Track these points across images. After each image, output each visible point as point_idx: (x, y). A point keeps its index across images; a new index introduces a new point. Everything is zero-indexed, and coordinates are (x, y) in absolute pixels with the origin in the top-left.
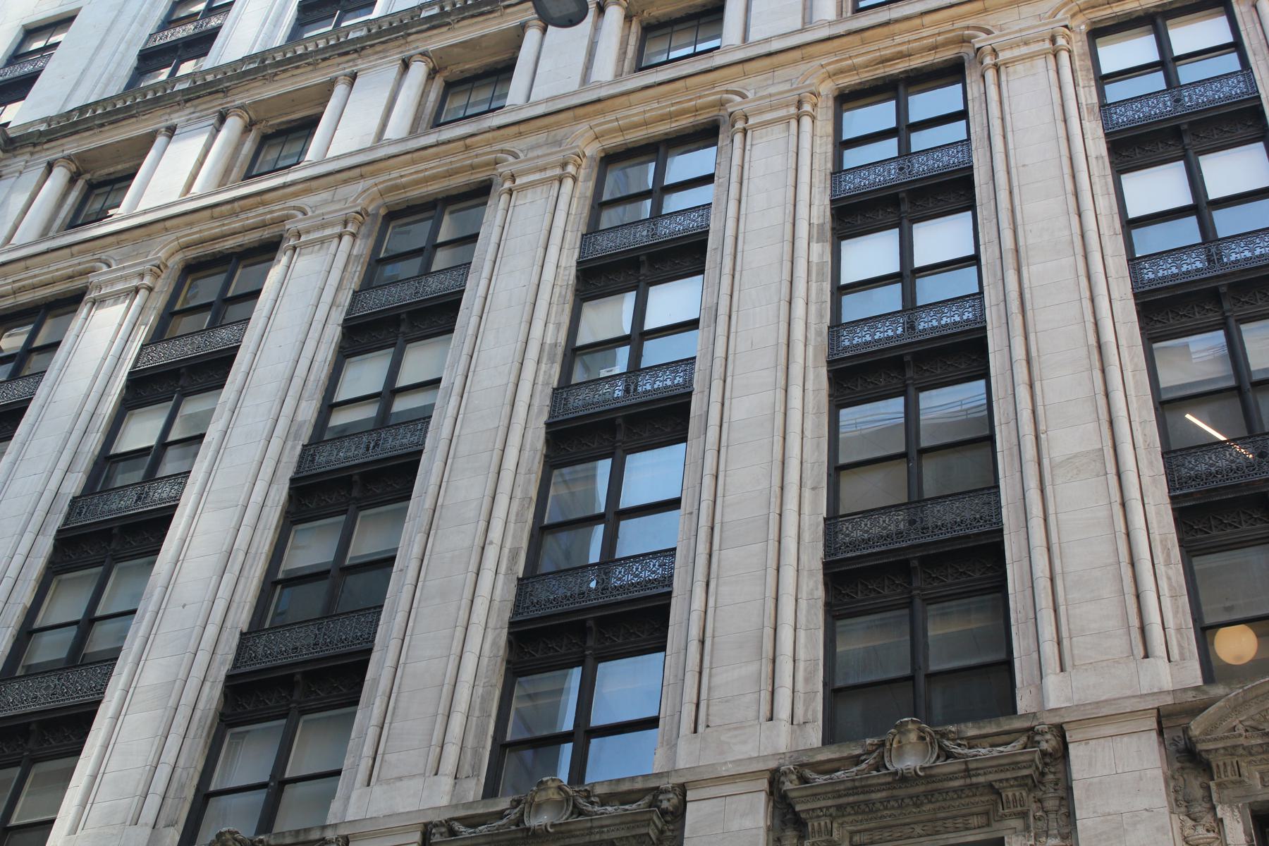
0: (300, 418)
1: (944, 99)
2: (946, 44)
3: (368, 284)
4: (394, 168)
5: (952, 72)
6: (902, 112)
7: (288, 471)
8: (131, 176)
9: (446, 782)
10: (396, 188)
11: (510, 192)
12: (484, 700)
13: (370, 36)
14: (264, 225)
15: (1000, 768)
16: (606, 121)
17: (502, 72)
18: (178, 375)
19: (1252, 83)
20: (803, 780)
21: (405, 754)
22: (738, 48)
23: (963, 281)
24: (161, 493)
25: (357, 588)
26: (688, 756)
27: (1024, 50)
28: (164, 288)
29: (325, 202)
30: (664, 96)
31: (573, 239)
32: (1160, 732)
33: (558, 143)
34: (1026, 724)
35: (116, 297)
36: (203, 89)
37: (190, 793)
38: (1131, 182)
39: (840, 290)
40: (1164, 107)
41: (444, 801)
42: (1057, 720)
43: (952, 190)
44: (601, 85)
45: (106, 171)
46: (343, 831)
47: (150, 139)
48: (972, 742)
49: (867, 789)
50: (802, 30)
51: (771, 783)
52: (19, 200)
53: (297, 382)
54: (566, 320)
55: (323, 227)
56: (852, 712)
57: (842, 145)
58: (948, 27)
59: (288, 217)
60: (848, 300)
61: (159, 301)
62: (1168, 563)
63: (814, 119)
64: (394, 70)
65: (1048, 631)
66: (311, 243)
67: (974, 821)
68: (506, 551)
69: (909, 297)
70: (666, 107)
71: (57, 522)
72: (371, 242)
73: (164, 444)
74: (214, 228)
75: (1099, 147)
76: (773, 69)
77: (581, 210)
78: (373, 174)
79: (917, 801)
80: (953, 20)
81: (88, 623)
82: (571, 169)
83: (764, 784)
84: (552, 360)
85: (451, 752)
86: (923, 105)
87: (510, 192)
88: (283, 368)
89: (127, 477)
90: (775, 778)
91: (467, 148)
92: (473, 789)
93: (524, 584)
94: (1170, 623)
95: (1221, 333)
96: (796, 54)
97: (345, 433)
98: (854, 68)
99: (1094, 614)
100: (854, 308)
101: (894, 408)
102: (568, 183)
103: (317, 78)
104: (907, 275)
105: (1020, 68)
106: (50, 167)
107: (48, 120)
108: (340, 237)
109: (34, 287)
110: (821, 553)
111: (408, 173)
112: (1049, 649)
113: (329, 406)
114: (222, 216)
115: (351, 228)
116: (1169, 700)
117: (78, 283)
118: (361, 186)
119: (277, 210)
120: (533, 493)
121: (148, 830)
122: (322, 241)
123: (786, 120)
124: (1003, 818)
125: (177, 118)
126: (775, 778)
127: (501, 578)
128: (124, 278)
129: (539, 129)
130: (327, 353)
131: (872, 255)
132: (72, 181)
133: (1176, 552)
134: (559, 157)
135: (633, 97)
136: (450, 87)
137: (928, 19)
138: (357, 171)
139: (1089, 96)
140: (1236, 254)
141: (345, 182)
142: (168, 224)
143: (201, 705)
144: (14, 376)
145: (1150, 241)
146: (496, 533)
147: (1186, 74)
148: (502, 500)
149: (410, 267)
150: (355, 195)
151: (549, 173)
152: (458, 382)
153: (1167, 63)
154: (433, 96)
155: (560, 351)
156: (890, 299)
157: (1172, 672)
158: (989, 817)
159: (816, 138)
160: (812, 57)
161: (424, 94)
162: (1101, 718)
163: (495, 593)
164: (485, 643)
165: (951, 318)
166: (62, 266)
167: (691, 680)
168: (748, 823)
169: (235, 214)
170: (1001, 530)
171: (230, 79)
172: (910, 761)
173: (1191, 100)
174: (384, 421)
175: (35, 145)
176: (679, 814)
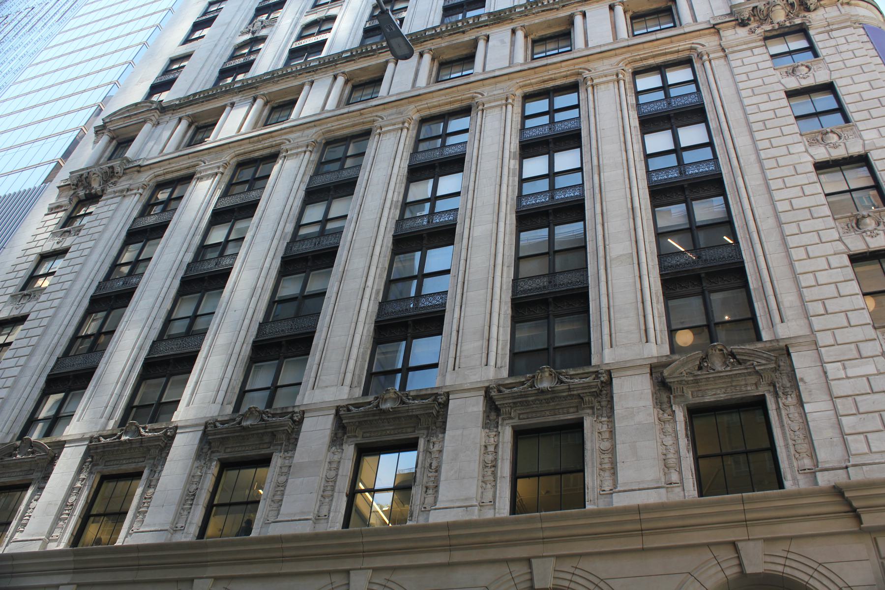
0: (286, 230)
1: (570, 99)
3: (317, 173)
5: (574, 87)
6: (551, 104)
7: (280, 254)
8: (215, 124)
9: (346, 389)
10: (330, 131)
11: (380, 134)
12: (364, 354)
13: (320, 65)
14: (272, 146)
15: (583, 388)
16: (422, 104)
17: (377, 81)
18: (234, 212)
19: (701, 97)
20: (499, 391)
21: (329, 376)
22: (481, 74)
23: (575, 179)
24: (226, 262)
25: (309, 305)
26: (450, 380)
27: (605, 79)
28: (228, 173)
29: (299, 137)
30: (448, 94)
31: (407, 155)
32: (651, 374)
33: (401, 113)
34: (595, 370)
35: (208, 177)
36: (247, 87)
37: (237, 391)
38: (649, 138)
39: (522, 181)
40: (664, 106)
41: (345, 397)
42: (608, 368)
43: (571, 139)
44: (420, 88)
46: (302, 408)
47: (223, 108)
48: (572, 377)
49: (526, 396)
50: (509, 67)
51: (486, 392)
52: (166, 134)
53: (285, 215)
54: (402, 190)
55: (298, 148)
56: (521, 363)
57: (525, 118)
58: (572, 68)
59: (282, 143)
60: (525, 185)
61: (226, 179)
62: (658, 302)
63: (513, 106)
64: (330, 79)
65: (606, 330)
66: (293, 155)
67: (572, 410)
68: (374, 291)
69: (552, 185)
71: (181, 274)
72: (318, 154)
73: (227, 241)
74: (250, 147)
75: (635, 123)
76: (496, 83)
77: (410, 143)
78: (320, 125)
79: (548, 401)
80: (574, 65)
81: (195, 317)
82: (406, 125)
83: (483, 393)
84: (396, 208)
85: (349, 376)
86: (561, 101)
87: (380, 134)
88: (279, 209)
89: (212, 255)
90: (487, 390)
91: (361, 114)
92: (358, 392)
93: (382, 305)
94: (658, 328)
95: (684, 205)
96: (506, 77)
97: (306, 238)
98: (531, 84)
99: (626, 323)
100: (528, 189)
101: (545, 232)
102: (405, 131)
103: (296, 83)
104: (551, 175)
105: (602, 86)
106: (180, 120)
107: (179, 99)
108: (305, 152)
109: (172, 172)
110: (510, 294)
111: (334, 125)
112: (606, 338)
113: (299, 226)
114: (253, 142)
115: (310, 148)
116: (655, 361)
117: (191, 171)
118: (314, 130)
119: (278, 140)
120: (387, 266)
121: (220, 406)
122: (297, 154)
123: (501, 106)
124: (584, 409)
125: (235, 99)
126: (487, 390)
127: (372, 302)
129: (392, 107)
130: (298, 202)
131: (536, 166)
132: (190, 126)
133: (661, 298)
134: (401, 119)
136: (355, 88)
137: (564, 64)
138: (313, 124)
139: (632, 100)
140: (692, 171)
141: (308, 128)
143: (242, 354)
144: (164, 210)
146: (370, 283)
147: (674, 92)
148: (373, 269)
149: (336, 166)
150: (312, 134)
151: (397, 126)
152: (355, 216)
153: (665, 87)
154: (347, 91)
155: (400, 204)
156: (544, 185)
157: (657, 349)
158: (578, 408)
159: (513, 114)
160: (513, 79)
161: (343, 91)
162: (627, 368)
163: (369, 309)
164: (364, 330)
165: (570, 194)
166: (185, 163)
167: (453, 348)
168: (475, 409)
170: (588, 287)
171: (258, 82)
172: (545, 384)
173: (675, 104)
174: (322, 233)
176: (446, 405)
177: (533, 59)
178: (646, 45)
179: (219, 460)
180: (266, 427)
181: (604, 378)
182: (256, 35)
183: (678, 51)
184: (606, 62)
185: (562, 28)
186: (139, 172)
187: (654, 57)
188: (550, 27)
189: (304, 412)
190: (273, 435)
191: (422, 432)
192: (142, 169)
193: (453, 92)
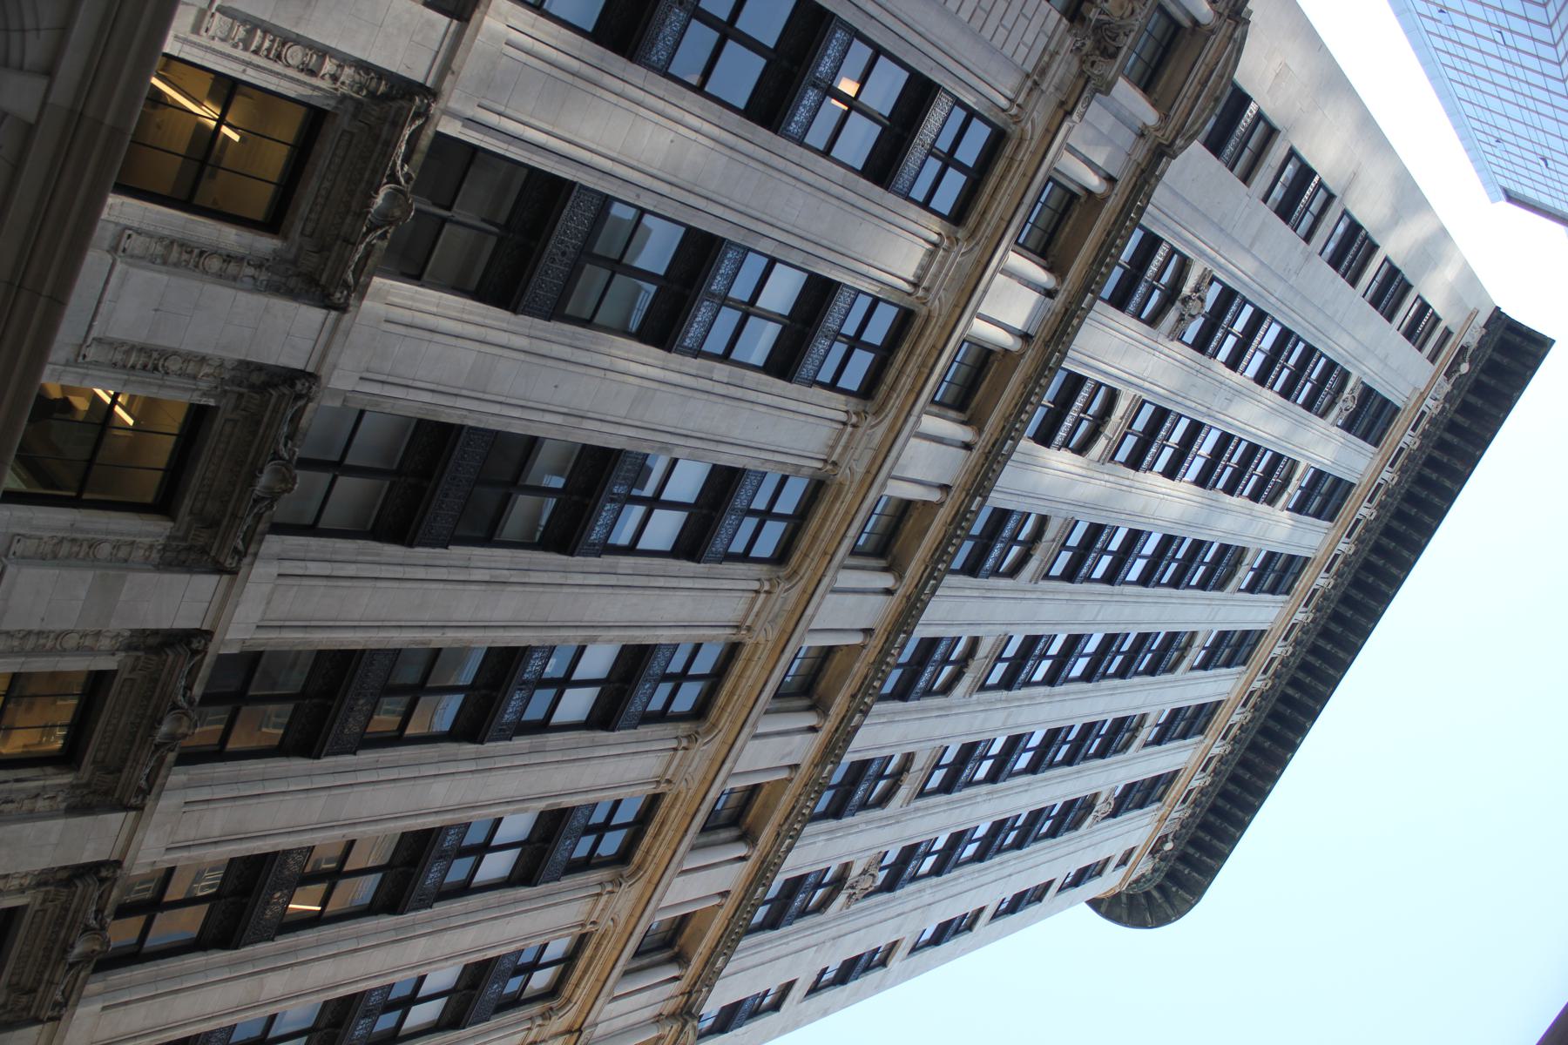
2: (644, 860)
4: (1030, 160)
14: (892, 388)
16: (763, 654)
45: (1074, 215)
51: (310, 374)
55: (845, 448)
60: (869, 52)
70: (746, 684)
78: (862, 481)
80: (657, 865)
90: (312, 377)
91: (825, 553)
95: (662, 272)
96: (710, 777)
109: (1002, 178)
114: (929, 354)
128: (936, 276)
129: (797, 604)
135: (766, 673)
137: (669, 853)
138: (874, 472)
140: (703, 313)
141: (875, 458)
142: (958, 310)
145: (754, 266)
160: (701, 783)
167: (325, 569)
169: (923, 364)
175: (1143, 171)
177: (1050, 179)
178: (616, 953)
179: (216, 408)
180: (234, 516)
181: (338, 296)
182: (1178, 304)
183: (577, 985)
184: (630, 904)
185: (895, 550)
186: (1062, 104)
187: (592, 959)
188: (765, 805)
189: (233, 573)
190: (213, 524)
191: (294, 250)
192: (1061, 113)
193: (748, 698)
